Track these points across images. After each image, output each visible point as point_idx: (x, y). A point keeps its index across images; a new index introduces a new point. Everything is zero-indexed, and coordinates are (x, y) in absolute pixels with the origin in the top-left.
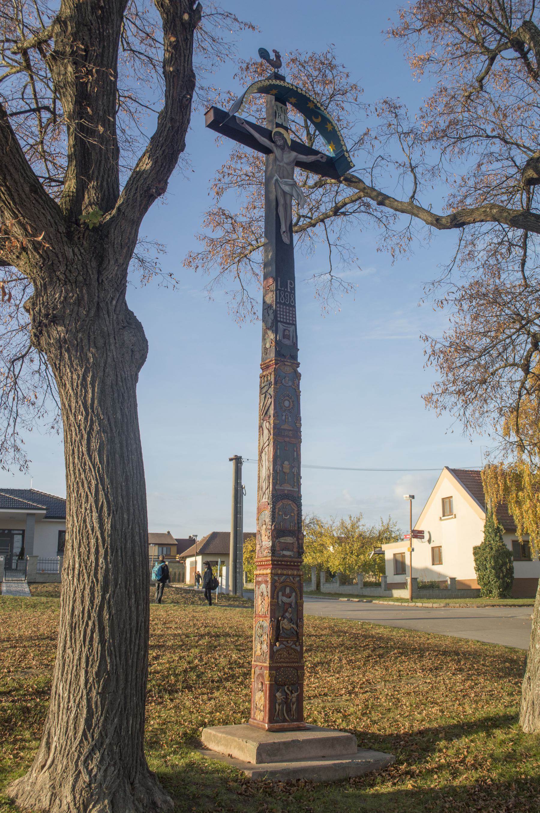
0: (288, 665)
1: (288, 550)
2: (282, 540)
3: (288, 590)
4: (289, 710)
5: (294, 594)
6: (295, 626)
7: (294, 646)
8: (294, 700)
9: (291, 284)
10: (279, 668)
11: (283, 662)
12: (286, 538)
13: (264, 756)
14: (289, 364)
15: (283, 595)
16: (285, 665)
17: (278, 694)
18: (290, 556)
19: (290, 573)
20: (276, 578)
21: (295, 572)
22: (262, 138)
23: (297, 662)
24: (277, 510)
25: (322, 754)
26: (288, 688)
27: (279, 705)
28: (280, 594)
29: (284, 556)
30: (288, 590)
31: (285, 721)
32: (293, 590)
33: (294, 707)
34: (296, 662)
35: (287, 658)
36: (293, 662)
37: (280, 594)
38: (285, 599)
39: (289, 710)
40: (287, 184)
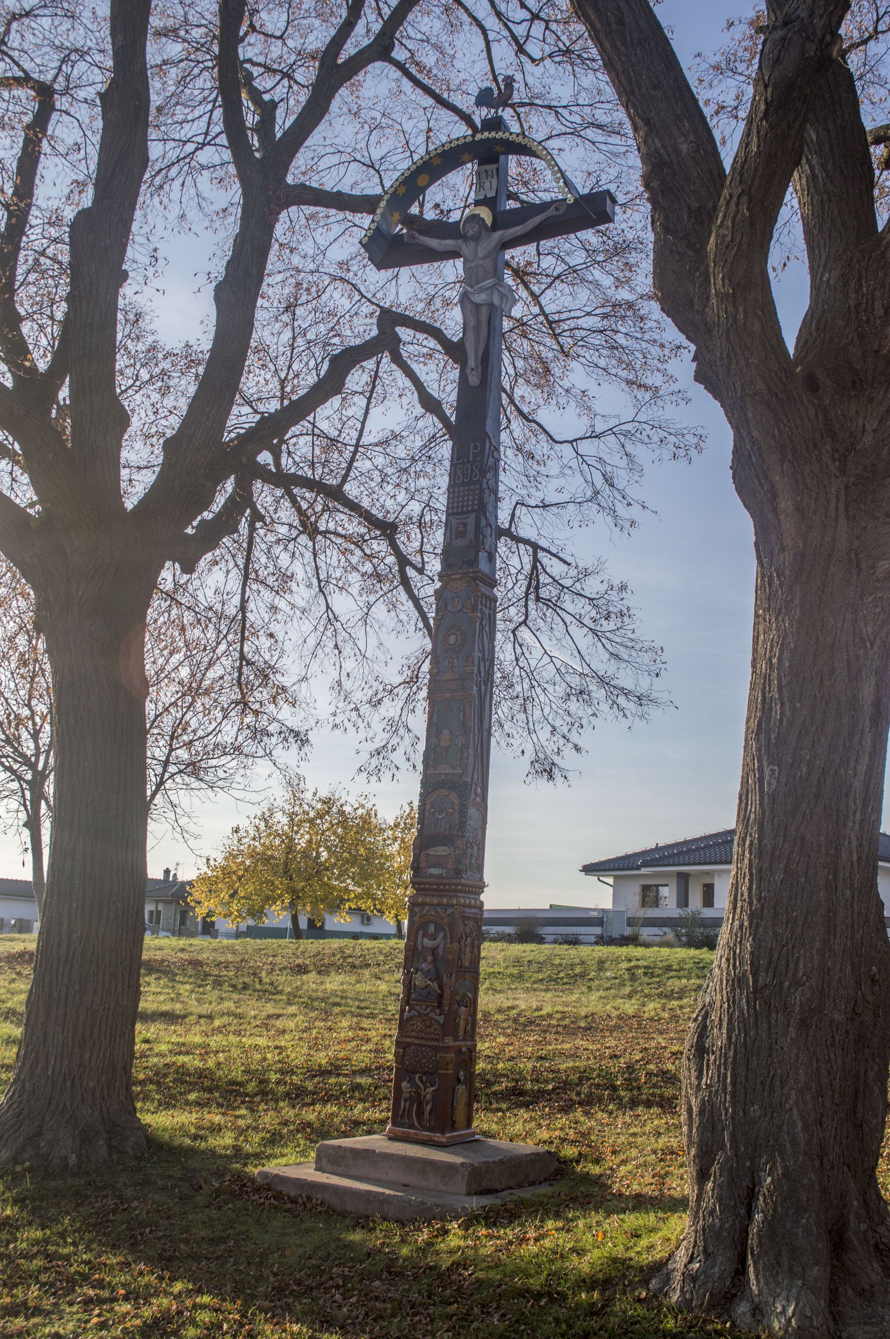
0: (423, 1042)
1: (434, 866)
2: (431, 852)
3: (432, 929)
4: (420, 1113)
5: (441, 935)
6: (435, 985)
7: (432, 1015)
8: (429, 1097)
9: (475, 447)
10: (410, 1045)
11: (415, 1037)
12: (437, 848)
13: (324, 1162)
14: (458, 576)
15: (423, 936)
16: (416, 1041)
17: (404, 1084)
18: (440, 876)
19: (435, 901)
20: (417, 909)
21: (445, 901)
22: (443, 242)
23: (438, 1040)
24: (428, 807)
25: (405, 1182)
26: (421, 1079)
27: (405, 1101)
28: (421, 933)
29: (431, 876)
30: (432, 929)
31: (412, 1126)
32: (439, 928)
33: (428, 1108)
34: (434, 1040)
35: (422, 1031)
36: (431, 1039)
37: (421, 933)
38: (426, 941)
39: (420, 1113)
40: (482, 290)
